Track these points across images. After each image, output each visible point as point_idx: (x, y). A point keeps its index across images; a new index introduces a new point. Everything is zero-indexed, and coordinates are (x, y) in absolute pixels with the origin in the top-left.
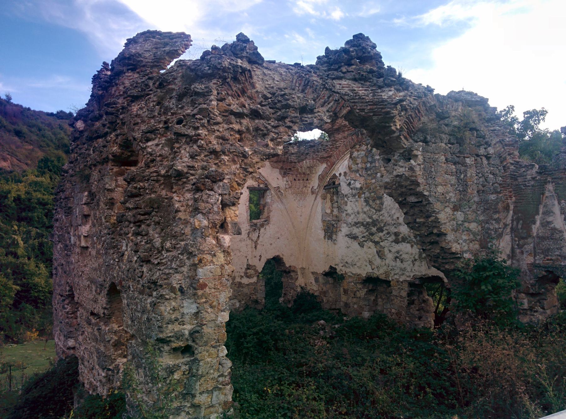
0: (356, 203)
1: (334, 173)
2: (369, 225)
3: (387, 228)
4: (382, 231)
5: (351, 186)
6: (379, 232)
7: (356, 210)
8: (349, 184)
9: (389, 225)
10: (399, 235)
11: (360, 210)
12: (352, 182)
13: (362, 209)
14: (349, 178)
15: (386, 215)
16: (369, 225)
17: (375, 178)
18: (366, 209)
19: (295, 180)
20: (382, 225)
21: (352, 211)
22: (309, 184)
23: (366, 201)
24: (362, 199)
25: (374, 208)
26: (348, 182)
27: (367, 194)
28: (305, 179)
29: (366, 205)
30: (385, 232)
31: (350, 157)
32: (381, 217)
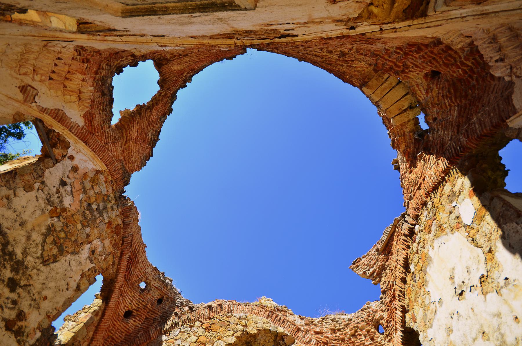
0: (38, 212)
1: (71, 142)
2: (11, 259)
3: (24, 294)
4: (12, 290)
5: (62, 190)
6: (8, 286)
7: (25, 216)
8: (63, 183)
9: (29, 292)
10: (21, 320)
11: (29, 226)
12: (68, 188)
13: (33, 229)
14: (73, 180)
15: (42, 277)
16: (11, 259)
17: (83, 226)
18: (37, 237)
19: (59, 58)
20: (22, 283)
21: (19, 209)
22: (41, 81)
23: (50, 229)
24: (49, 222)
25: (43, 250)
26: (66, 179)
27: (58, 225)
28: (53, 76)
29: (43, 234)
30: (14, 296)
31: (98, 172)
32: (35, 271)
